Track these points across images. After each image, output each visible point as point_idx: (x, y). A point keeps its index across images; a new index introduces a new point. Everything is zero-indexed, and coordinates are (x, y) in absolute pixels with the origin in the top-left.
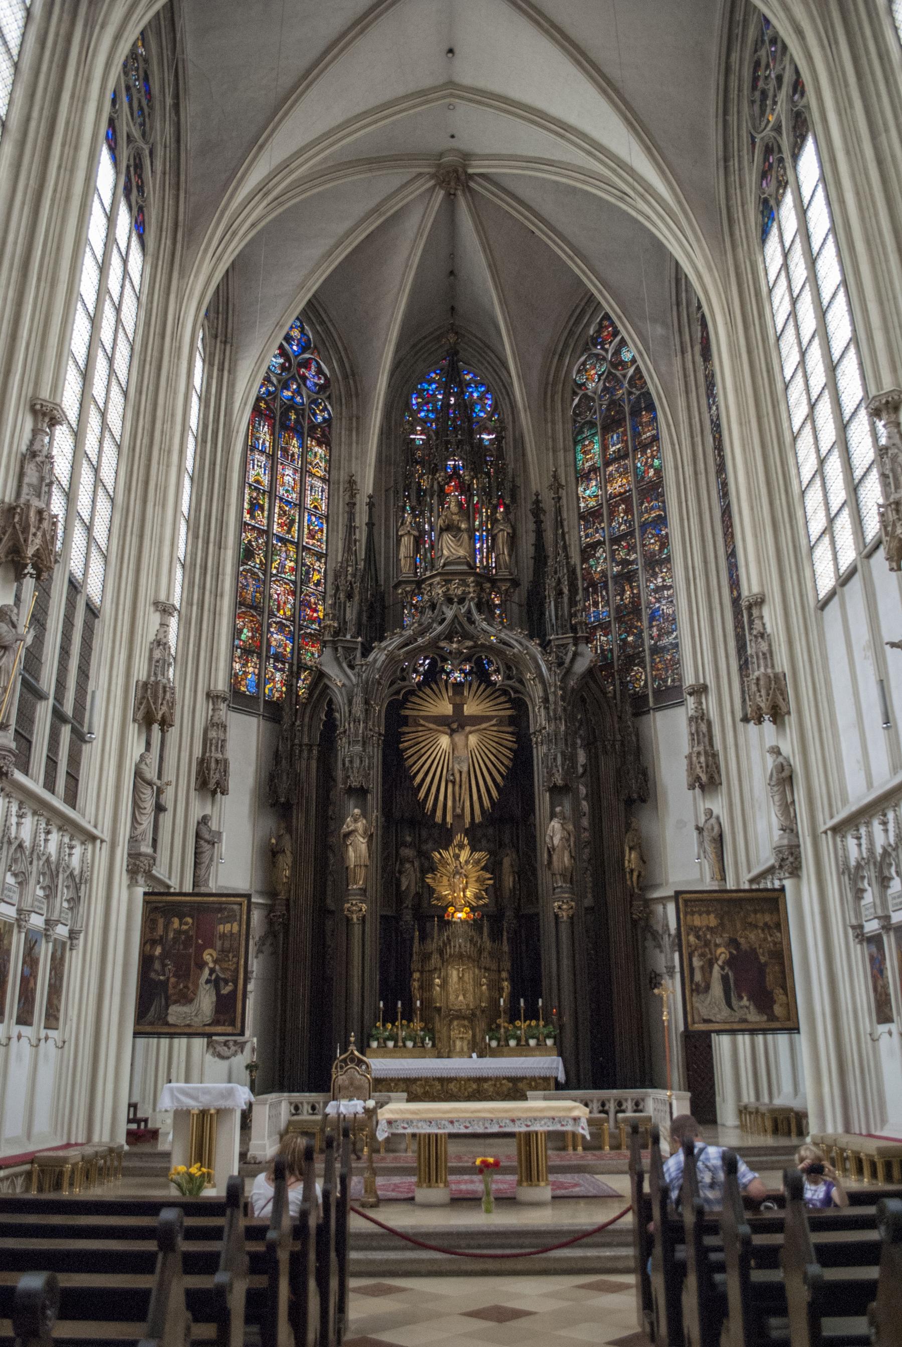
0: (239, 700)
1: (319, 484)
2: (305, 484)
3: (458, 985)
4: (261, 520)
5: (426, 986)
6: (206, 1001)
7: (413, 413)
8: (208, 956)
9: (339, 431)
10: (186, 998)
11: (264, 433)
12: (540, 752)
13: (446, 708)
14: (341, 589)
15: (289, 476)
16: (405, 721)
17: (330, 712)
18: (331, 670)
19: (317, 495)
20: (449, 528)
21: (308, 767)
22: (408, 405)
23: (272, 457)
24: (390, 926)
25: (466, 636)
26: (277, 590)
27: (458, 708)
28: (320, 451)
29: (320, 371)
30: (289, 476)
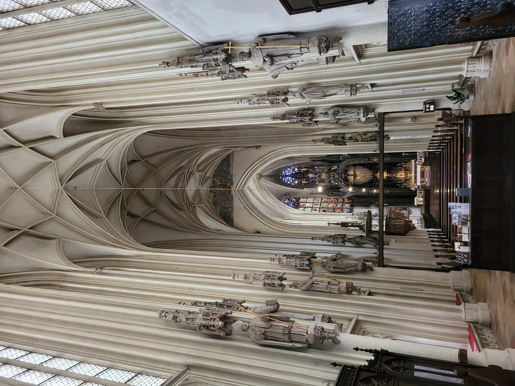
0: (351, 211)
1: (308, 200)
2: (309, 202)
3: (401, 175)
4: (318, 209)
5: (401, 180)
6: (404, 211)
7: (291, 183)
8: (397, 211)
9: (297, 196)
10: (404, 214)
11: (301, 209)
12: (362, 162)
13: (352, 177)
14: (333, 195)
15: (308, 205)
16: (354, 184)
17: (354, 196)
18: (347, 196)
19: (311, 200)
20: (320, 176)
21: (363, 200)
22: (290, 184)
23: (305, 208)
24: (389, 187)
25: (341, 174)
26: (330, 206)
27: (352, 175)
28: (301, 200)
29: (285, 200)
30: (308, 205)
